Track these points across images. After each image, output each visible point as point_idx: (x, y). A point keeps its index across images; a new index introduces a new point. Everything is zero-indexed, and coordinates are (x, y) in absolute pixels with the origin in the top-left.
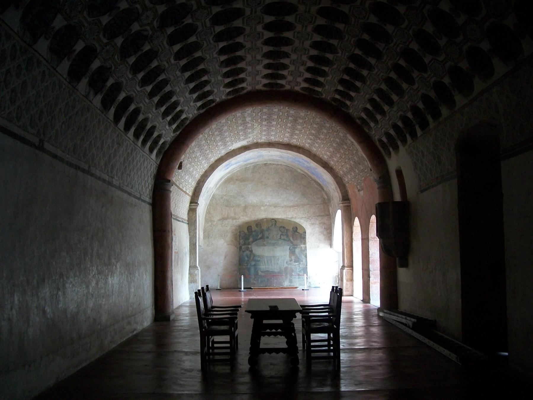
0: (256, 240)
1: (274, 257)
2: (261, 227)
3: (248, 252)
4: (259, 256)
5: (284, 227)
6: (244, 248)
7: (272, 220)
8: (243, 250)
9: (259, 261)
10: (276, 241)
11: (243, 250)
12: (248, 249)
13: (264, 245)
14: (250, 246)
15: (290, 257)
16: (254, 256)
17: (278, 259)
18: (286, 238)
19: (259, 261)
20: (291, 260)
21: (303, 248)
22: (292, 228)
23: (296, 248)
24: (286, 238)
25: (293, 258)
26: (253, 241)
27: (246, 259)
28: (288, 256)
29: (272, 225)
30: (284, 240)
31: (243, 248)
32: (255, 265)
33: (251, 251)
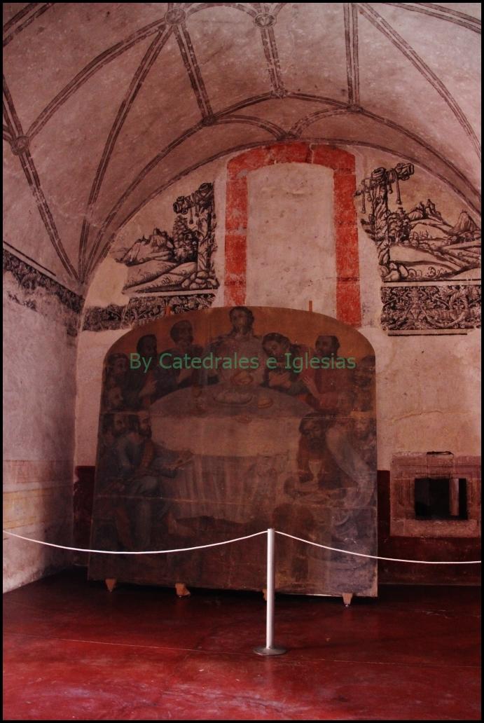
0: (170, 390)
1: (235, 460)
2: (191, 339)
3: (132, 437)
4: (174, 454)
5: (281, 339)
6: (120, 422)
7: (236, 313)
8: (117, 427)
9: (174, 475)
10: (245, 396)
11: (117, 427)
12: (133, 423)
13: (199, 412)
14: (142, 414)
15: (302, 462)
16: (157, 451)
17: (251, 468)
18: (288, 384)
19: (174, 475)
20: (305, 478)
21: (361, 427)
22: (317, 343)
23: (330, 424)
24: (288, 384)
25: (315, 466)
26: (155, 397)
27: (125, 463)
28: (293, 456)
29: (235, 330)
30: (280, 388)
31: (116, 418)
32: (157, 491)
33: (147, 434)
